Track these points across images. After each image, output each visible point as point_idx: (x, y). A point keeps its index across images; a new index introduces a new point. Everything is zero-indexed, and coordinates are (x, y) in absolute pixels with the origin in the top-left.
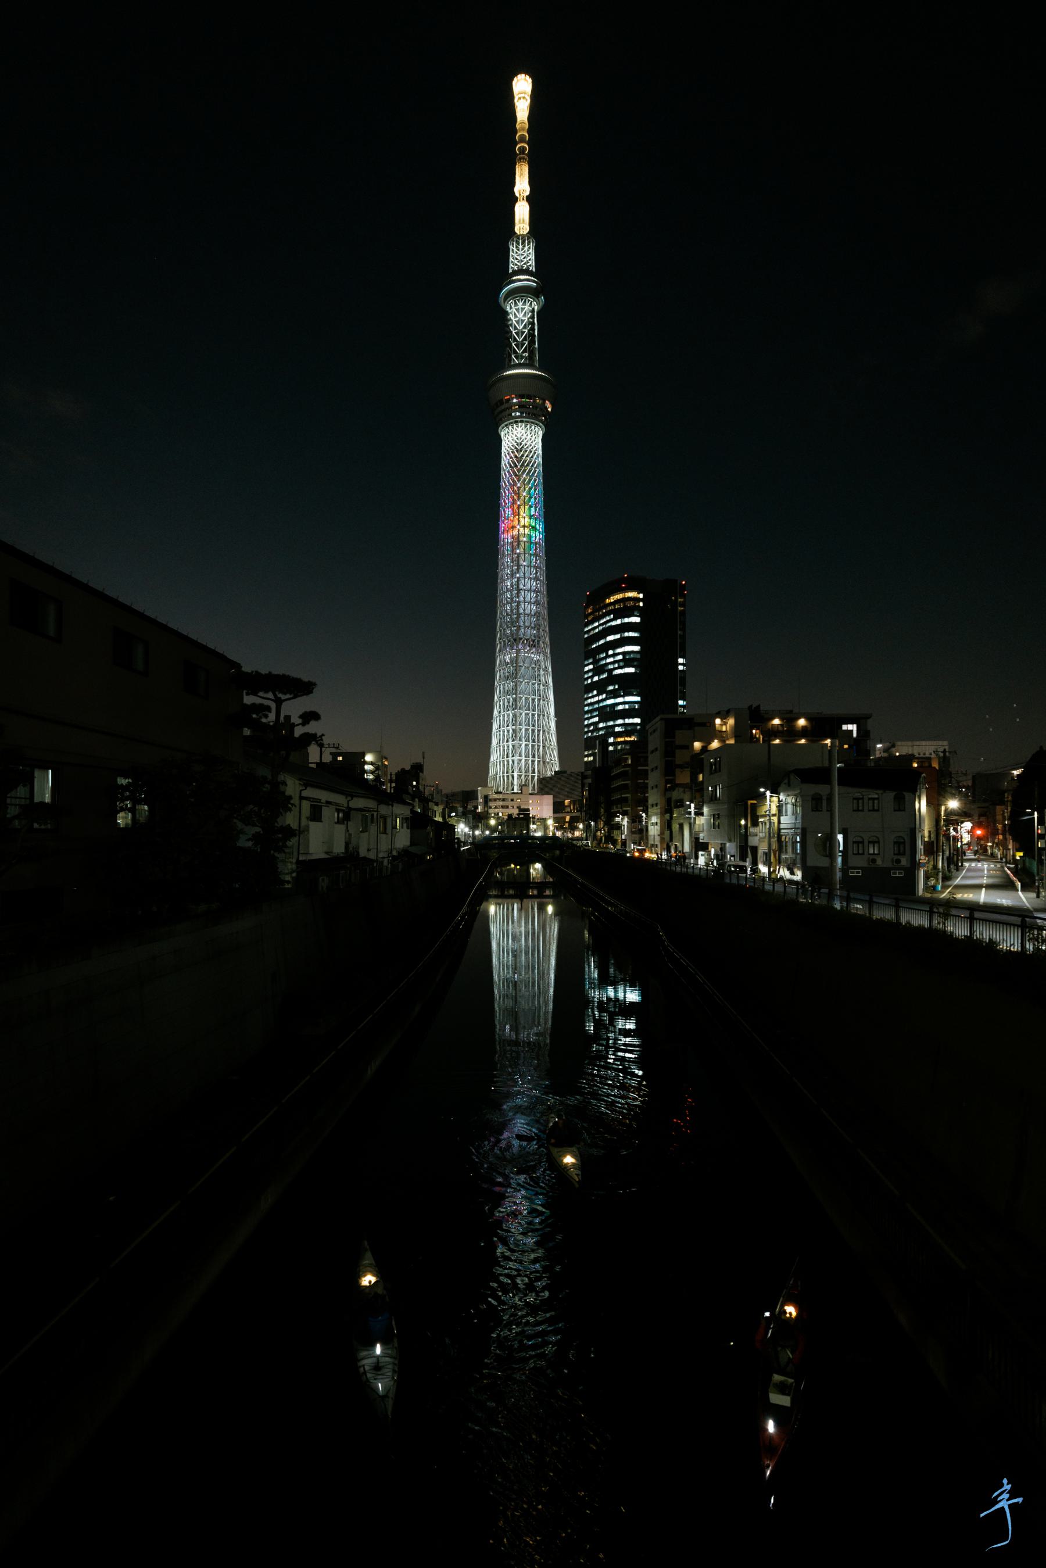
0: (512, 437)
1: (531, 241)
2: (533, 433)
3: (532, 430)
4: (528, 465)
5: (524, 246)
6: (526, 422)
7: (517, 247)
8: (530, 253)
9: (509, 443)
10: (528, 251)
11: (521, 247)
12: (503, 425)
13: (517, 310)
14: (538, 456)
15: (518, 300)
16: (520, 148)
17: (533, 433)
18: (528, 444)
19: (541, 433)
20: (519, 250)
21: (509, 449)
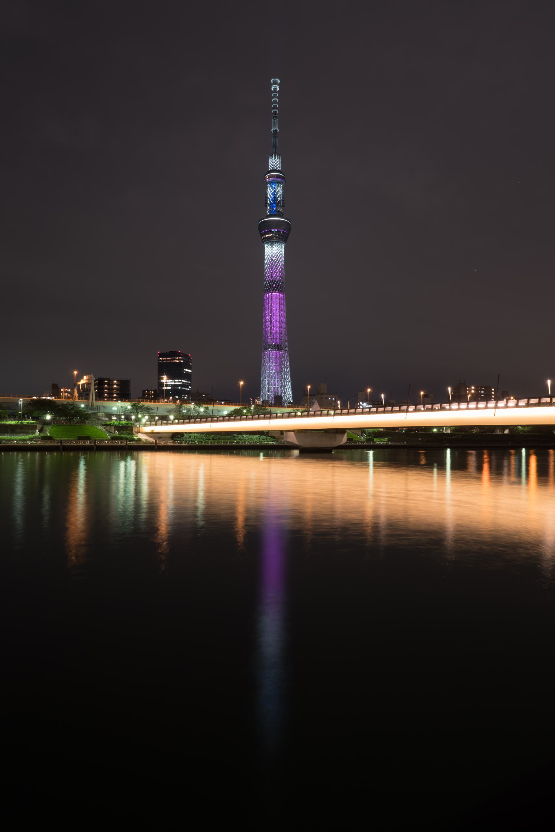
0: (269, 248)
1: (279, 155)
2: (279, 247)
3: (278, 245)
4: (276, 262)
5: (275, 158)
6: (275, 241)
7: (272, 159)
8: (278, 161)
9: (267, 251)
10: (277, 160)
11: (273, 158)
12: (265, 243)
13: (272, 188)
14: (282, 256)
15: (272, 184)
16: (274, 111)
17: (279, 247)
18: (276, 252)
19: (283, 246)
20: (272, 160)
21: (267, 254)
